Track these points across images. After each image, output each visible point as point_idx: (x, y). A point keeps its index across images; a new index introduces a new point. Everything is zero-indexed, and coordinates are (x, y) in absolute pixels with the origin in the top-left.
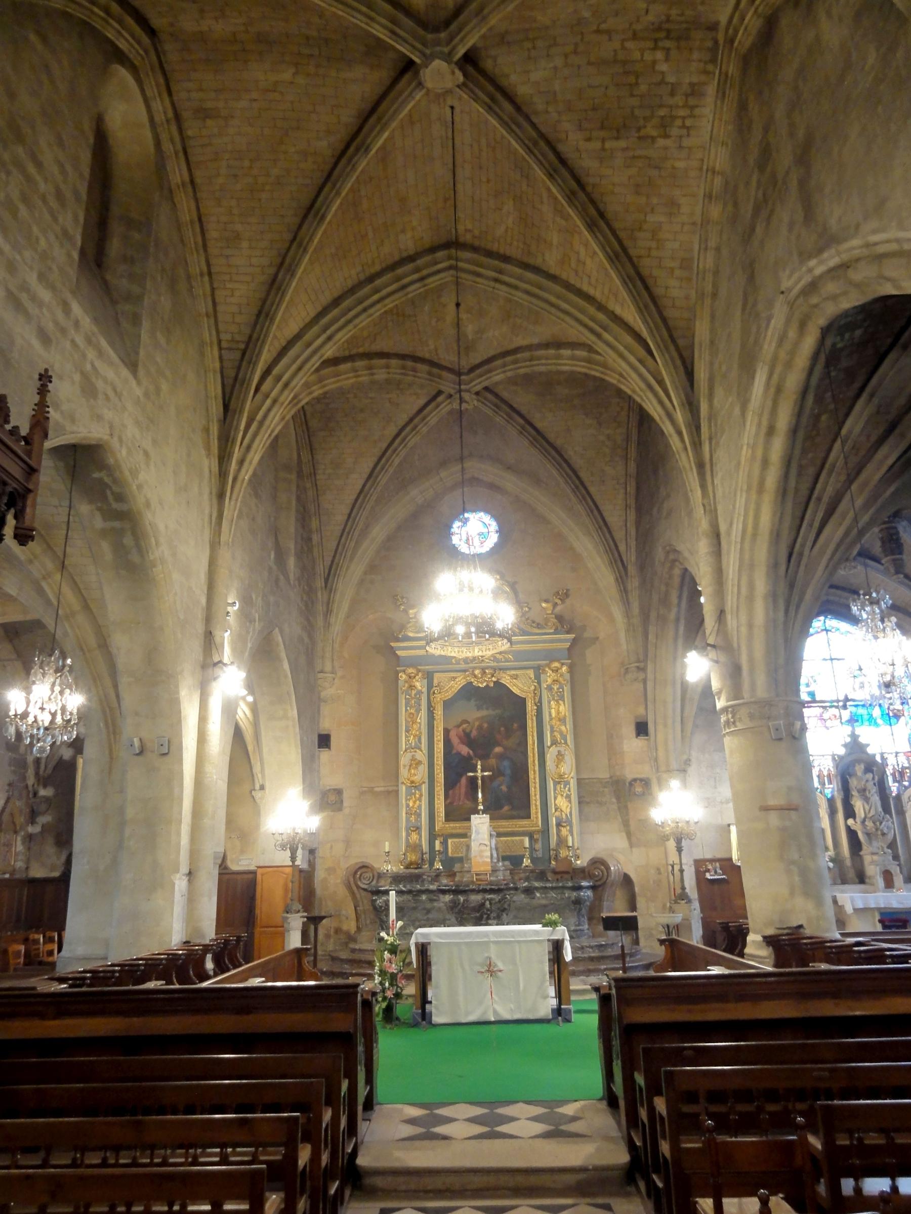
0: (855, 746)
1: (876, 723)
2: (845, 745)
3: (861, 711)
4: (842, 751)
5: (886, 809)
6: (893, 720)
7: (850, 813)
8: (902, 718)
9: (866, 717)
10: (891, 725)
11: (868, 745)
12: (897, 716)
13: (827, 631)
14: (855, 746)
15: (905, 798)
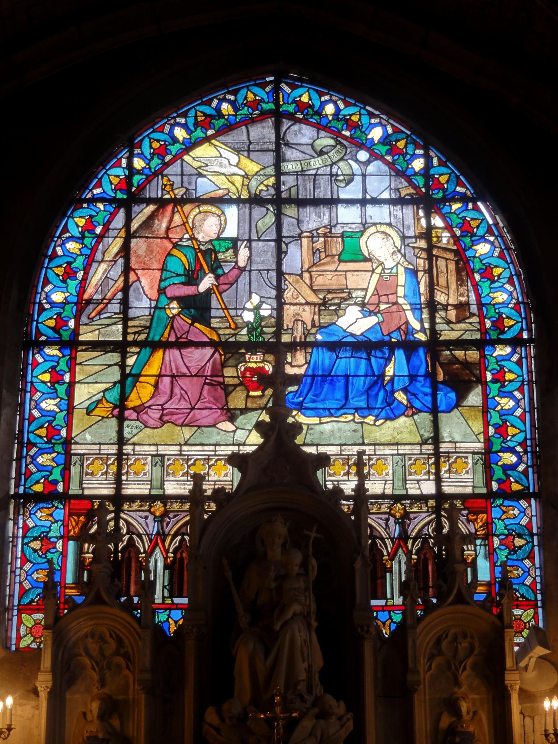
0: (282, 465)
1: (390, 400)
2: (235, 460)
3: (345, 364)
4: (225, 477)
5: (340, 675)
6: (446, 396)
7: (217, 685)
8: (474, 398)
9: (360, 383)
10: (435, 411)
11: (323, 461)
12: (461, 389)
13: (278, 116)
14: (282, 465)
15: (423, 639)
